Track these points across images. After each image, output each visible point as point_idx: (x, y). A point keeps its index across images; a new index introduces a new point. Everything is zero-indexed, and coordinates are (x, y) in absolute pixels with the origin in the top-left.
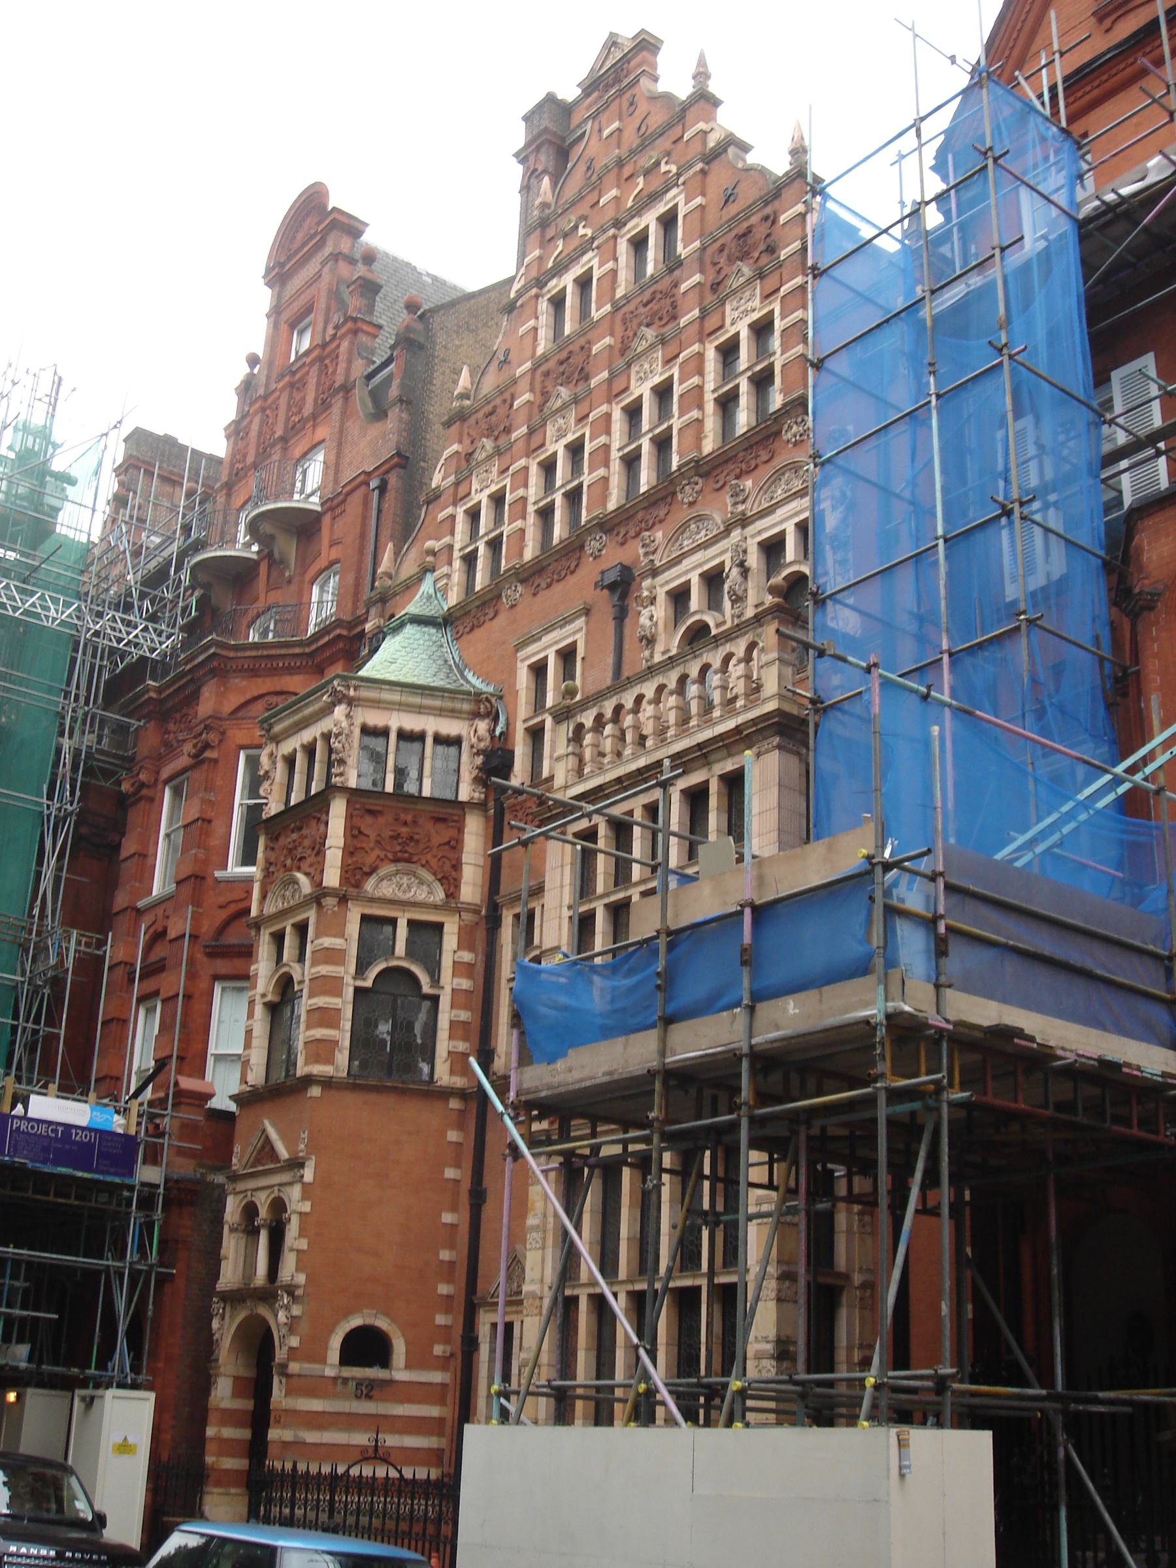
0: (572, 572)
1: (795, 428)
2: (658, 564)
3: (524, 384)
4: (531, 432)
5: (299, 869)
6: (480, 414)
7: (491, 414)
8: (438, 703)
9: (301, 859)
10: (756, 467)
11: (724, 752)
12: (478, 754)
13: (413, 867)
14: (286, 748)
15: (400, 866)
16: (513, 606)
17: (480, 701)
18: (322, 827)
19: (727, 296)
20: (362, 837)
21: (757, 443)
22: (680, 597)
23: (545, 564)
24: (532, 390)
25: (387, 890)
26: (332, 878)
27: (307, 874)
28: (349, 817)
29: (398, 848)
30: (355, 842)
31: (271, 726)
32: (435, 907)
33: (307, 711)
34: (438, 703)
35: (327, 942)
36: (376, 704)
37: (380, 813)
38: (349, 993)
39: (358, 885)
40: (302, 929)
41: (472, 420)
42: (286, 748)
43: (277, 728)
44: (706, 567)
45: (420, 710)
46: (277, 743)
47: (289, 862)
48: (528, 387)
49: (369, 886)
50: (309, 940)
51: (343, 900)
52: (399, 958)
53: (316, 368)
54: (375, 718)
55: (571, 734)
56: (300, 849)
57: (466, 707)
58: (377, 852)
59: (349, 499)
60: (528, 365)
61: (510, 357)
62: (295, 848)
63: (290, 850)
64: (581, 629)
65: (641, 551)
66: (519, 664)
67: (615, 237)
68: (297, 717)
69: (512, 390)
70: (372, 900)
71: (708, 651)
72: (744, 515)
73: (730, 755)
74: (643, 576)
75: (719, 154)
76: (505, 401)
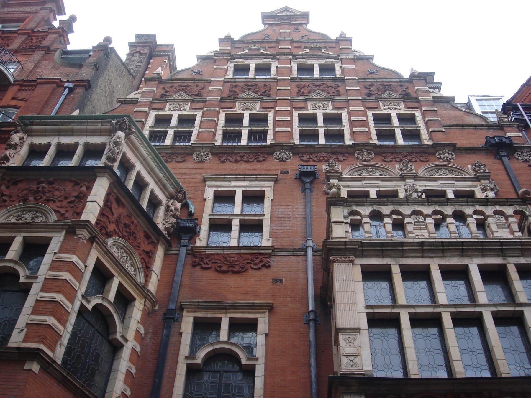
0: (259, 161)
1: (447, 155)
2: (344, 176)
8: (161, 175)
10: (416, 161)
11: (519, 253)
12: (173, 216)
13: (133, 250)
17: (180, 192)
19: (381, 100)
21: (416, 153)
31: (32, 124)
32: (136, 285)
34: (161, 175)
36: (134, 149)
37: (123, 205)
44: (381, 189)
45: (151, 171)
51: (92, 240)
53: (24, 37)
55: (346, 214)
57: (171, 189)
59: (38, 86)
64: (270, 187)
66: (206, 187)
71: (480, 205)
73: (523, 256)
74: (328, 179)
75: (363, 59)
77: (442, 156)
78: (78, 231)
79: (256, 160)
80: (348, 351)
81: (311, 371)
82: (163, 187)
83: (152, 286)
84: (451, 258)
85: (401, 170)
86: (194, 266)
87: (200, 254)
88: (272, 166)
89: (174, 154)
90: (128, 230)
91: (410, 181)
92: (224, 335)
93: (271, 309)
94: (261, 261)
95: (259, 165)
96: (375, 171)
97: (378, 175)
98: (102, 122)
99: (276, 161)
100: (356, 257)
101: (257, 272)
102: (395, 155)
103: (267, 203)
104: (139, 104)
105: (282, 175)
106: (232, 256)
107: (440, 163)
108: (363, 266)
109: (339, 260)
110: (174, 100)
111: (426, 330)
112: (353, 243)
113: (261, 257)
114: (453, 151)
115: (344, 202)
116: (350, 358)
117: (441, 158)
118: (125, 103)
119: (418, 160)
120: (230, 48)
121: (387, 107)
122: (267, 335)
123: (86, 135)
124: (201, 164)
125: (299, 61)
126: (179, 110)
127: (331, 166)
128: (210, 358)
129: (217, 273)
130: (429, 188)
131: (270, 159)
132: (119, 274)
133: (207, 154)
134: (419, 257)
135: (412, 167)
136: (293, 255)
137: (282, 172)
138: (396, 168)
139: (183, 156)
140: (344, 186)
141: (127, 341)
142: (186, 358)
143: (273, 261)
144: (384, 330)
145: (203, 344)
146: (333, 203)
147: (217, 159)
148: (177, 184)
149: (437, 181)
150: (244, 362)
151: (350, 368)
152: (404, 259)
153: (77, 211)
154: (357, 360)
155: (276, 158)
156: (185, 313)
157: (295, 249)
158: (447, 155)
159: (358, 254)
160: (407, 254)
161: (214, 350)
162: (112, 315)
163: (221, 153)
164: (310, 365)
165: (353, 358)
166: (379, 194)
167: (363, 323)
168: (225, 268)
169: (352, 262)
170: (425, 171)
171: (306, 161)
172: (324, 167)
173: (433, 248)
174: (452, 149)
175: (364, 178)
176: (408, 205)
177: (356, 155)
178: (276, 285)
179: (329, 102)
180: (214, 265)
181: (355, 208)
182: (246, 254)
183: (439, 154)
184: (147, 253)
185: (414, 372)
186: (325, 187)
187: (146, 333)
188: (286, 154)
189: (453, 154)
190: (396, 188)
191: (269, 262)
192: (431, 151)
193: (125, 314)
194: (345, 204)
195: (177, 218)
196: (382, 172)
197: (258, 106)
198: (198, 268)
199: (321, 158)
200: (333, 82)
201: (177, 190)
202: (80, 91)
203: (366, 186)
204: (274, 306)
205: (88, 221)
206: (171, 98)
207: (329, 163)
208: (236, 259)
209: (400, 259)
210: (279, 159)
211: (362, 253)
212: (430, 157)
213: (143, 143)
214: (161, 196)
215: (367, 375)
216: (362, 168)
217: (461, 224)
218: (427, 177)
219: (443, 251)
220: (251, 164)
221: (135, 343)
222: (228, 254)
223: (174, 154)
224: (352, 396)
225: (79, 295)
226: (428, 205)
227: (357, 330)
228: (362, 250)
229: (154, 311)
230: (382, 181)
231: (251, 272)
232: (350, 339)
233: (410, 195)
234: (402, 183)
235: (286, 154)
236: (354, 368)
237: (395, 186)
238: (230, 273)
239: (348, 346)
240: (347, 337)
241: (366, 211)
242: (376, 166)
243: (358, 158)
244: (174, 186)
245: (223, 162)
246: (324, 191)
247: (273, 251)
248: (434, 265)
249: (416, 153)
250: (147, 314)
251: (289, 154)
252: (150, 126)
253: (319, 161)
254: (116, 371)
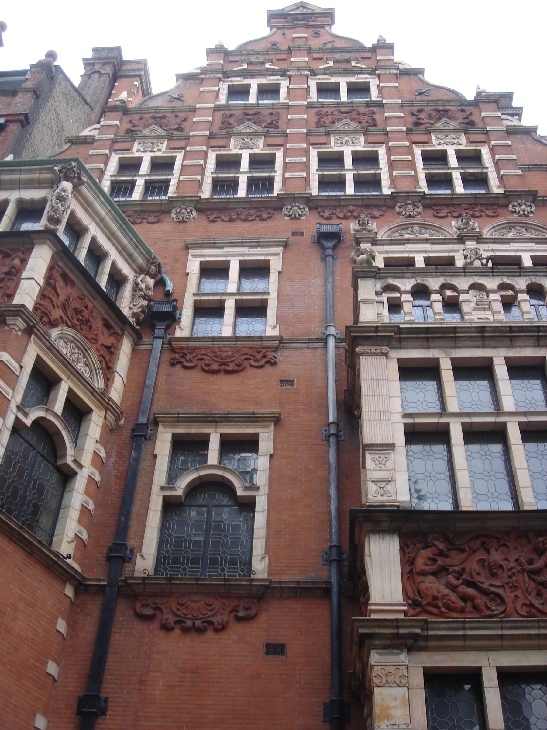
0: (262, 220)
1: (523, 207)
2: (380, 238)
8: (125, 241)
10: (481, 216)
12: (144, 298)
13: (87, 344)
16: (184, 222)
17: (153, 263)
19: (434, 131)
23: (230, 206)
25: (64, 349)
32: (93, 391)
34: (125, 241)
36: (87, 205)
37: (73, 283)
44: (431, 255)
45: (111, 236)
51: (29, 331)
64: (277, 254)
66: (190, 257)
67: (307, 76)
72: (481, 235)
74: (358, 242)
77: (517, 209)
78: (10, 320)
79: (258, 218)
80: (378, 475)
81: (330, 503)
82: (129, 258)
83: (116, 394)
84: (522, 349)
85: (459, 229)
86: (173, 365)
87: (181, 348)
88: (281, 226)
89: (145, 212)
90: (80, 317)
91: (471, 244)
92: (213, 457)
93: (277, 421)
94: (264, 357)
95: (262, 225)
96: (424, 231)
97: (427, 236)
98: (40, 169)
99: (286, 218)
100: (390, 348)
101: (259, 371)
102: (452, 209)
103: (273, 276)
104: (95, 144)
105: (294, 238)
106: (225, 349)
107: (515, 218)
108: (400, 360)
109: (368, 353)
110: (145, 137)
111: (485, 447)
112: (388, 329)
113: (264, 351)
114: (533, 202)
115: (377, 273)
116: (380, 484)
117: (515, 212)
118: (76, 144)
119: (483, 214)
120: (222, 62)
121: (442, 141)
122: (271, 456)
123: (20, 189)
124: (182, 225)
125: (320, 79)
126: (151, 151)
127: (363, 224)
128: (194, 489)
129: (203, 374)
130: (498, 254)
131: (277, 216)
132: (68, 377)
133: (191, 211)
134: (478, 347)
135: (475, 224)
136: (308, 347)
137: (294, 234)
138: (453, 226)
139: (157, 214)
140: (380, 252)
141: (81, 466)
142: (162, 488)
143: (280, 356)
144: (427, 447)
145: (184, 469)
146: (361, 274)
147: (204, 217)
148: (149, 252)
149: (509, 243)
150: (240, 492)
151: (380, 498)
152: (457, 350)
153: (8, 292)
154: (389, 487)
155: (286, 215)
156: (161, 428)
157: (311, 339)
158: (523, 207)
159: (394, 343)
160: (462, 344)
161: (200, 477)
162: (59, 433)
163: (209, 210)
164: (329, 497)
165: (384, 484)
166: (428, 261)
167: (400, 438)
168: (215, 367)
169: (386, 355)
170: (493, 230)
171: (328, 218)
172: (353, 226)
173: (497, 334)
174: (531, 199)
175: (408, 240)
176: (465, 276)
177: (397, 209)
178: (285, 389)
179: (360, 136)
180: (200, 362)
181: (391, 281)
182: (243, 347)
183: (513, 206)
184: (108, 348)
185: (467, 503)
186: (353, 254)
187: (108, 455)
188: (300, 209)
189: (533, 205)
190: (451, 254)
191: (275, 358)
192: (501, 202)
193: (79, 430)
194: (378, 275)
195: (150, 300)
196: (433, 232)
197: (261, 142)
198: (178, 367)
199: (349, 214)
200: (366, 106)
201: (149, 261)
202: (14, 128)
203: (410, 252)
204: (282, 417)
205: (23, 306)
206: (141, 135)
207: (359, 221)
208: (230, 353)
209: (452, 350)
210: (291, 215)
211: (400, 342)
212: (500, 211)
213: (98, 197)
214: (126, 269)
215: (403, 507)
216: (405, 227)
217: (542, 303)
218: (494, 239)
219: (511, 338)
221: (92, 469)
222: (219, 348)
223: (145, 212)
224: (381, 535)
225: (13, 406)
226: (493, 276)
227: (391, 447)
228: (400, 338)
229: (119, 427)
230: (432, 244)
231: (251, 372)
232: (380, 459)
233: (471, 263)
234: (461, 247)
235: (300, 209)
236: (385, 498)
237: (451, 251)
238: (222, 373)
239: (378, 468)
240: (377, 456)
241: (407, 284)
242: (424, 224)
243: (399, 213)
244: (144, 255)
245: (213, 221)
246: (352, 258)
247: (281, 343)
248: (499, 358)
249: (481, 205)
250: (110, 431)
251: (304, 208)
252: (112, 174)
253: (346, 218)
254: (68, 507)
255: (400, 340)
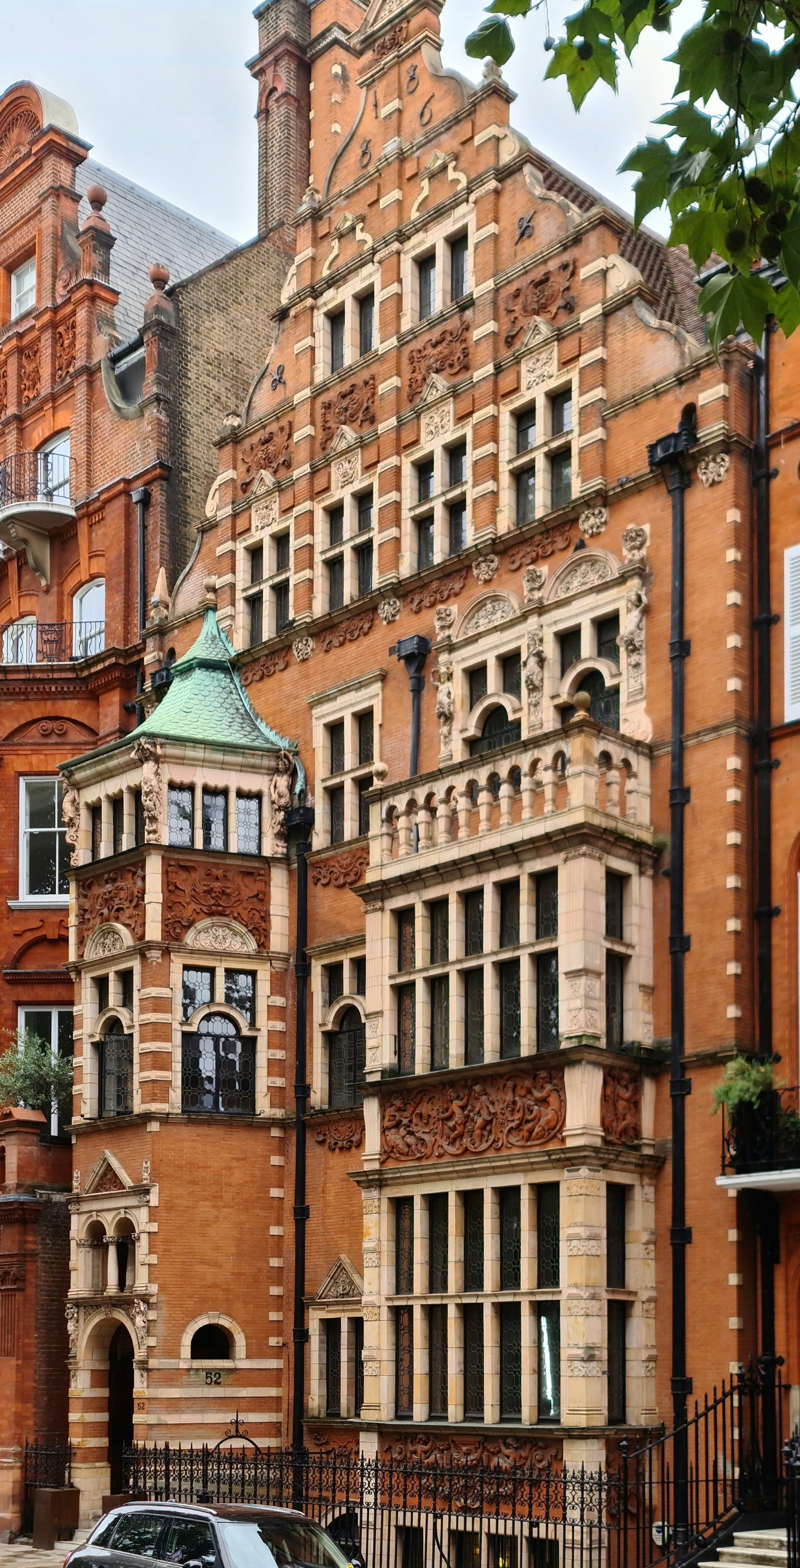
3: (302, 415)
4: (314, 472)
5: (117, 919)
6: (255, 439)
7: (267, 441)
9: (118, 910)
14: (90, 795)
15: (215, 919)
18: (139, 883)
20: (178, 893)
22: (476, 676)
24: (313, 423)
26: (154, 932)
27: (127, 926)
28: (165, 873)
29: (212, 902)
30: (173, 898)
31: (72, 773)
33: (111, 764)
35: (154, 991)
36: (181, 761)
38: (177, 1038)
39: (178, 938)
40: (126, 977)
41: (247, 444)
42: (90, 795)
43: (79, 776)
46: (79, 790)
47: (105, 911)
48: (308, 419)
49: (189, 938)
50: (135, 988)
51: (166, 952)
52: (220, 1004)
54: (182, 775)
56: (117, 901)
58: (193, 906)
60: (307, 392)
61: (285, 377)
62: (111, 899)
63: (106, 900)
65: (437, 624)
68: (100, 768)
69: (289, 418)
70: (193, 952)
74: (439, 651)
76: (282, 429)
169: (382, 909)
220: (356, 643)
255: (389, 890)
